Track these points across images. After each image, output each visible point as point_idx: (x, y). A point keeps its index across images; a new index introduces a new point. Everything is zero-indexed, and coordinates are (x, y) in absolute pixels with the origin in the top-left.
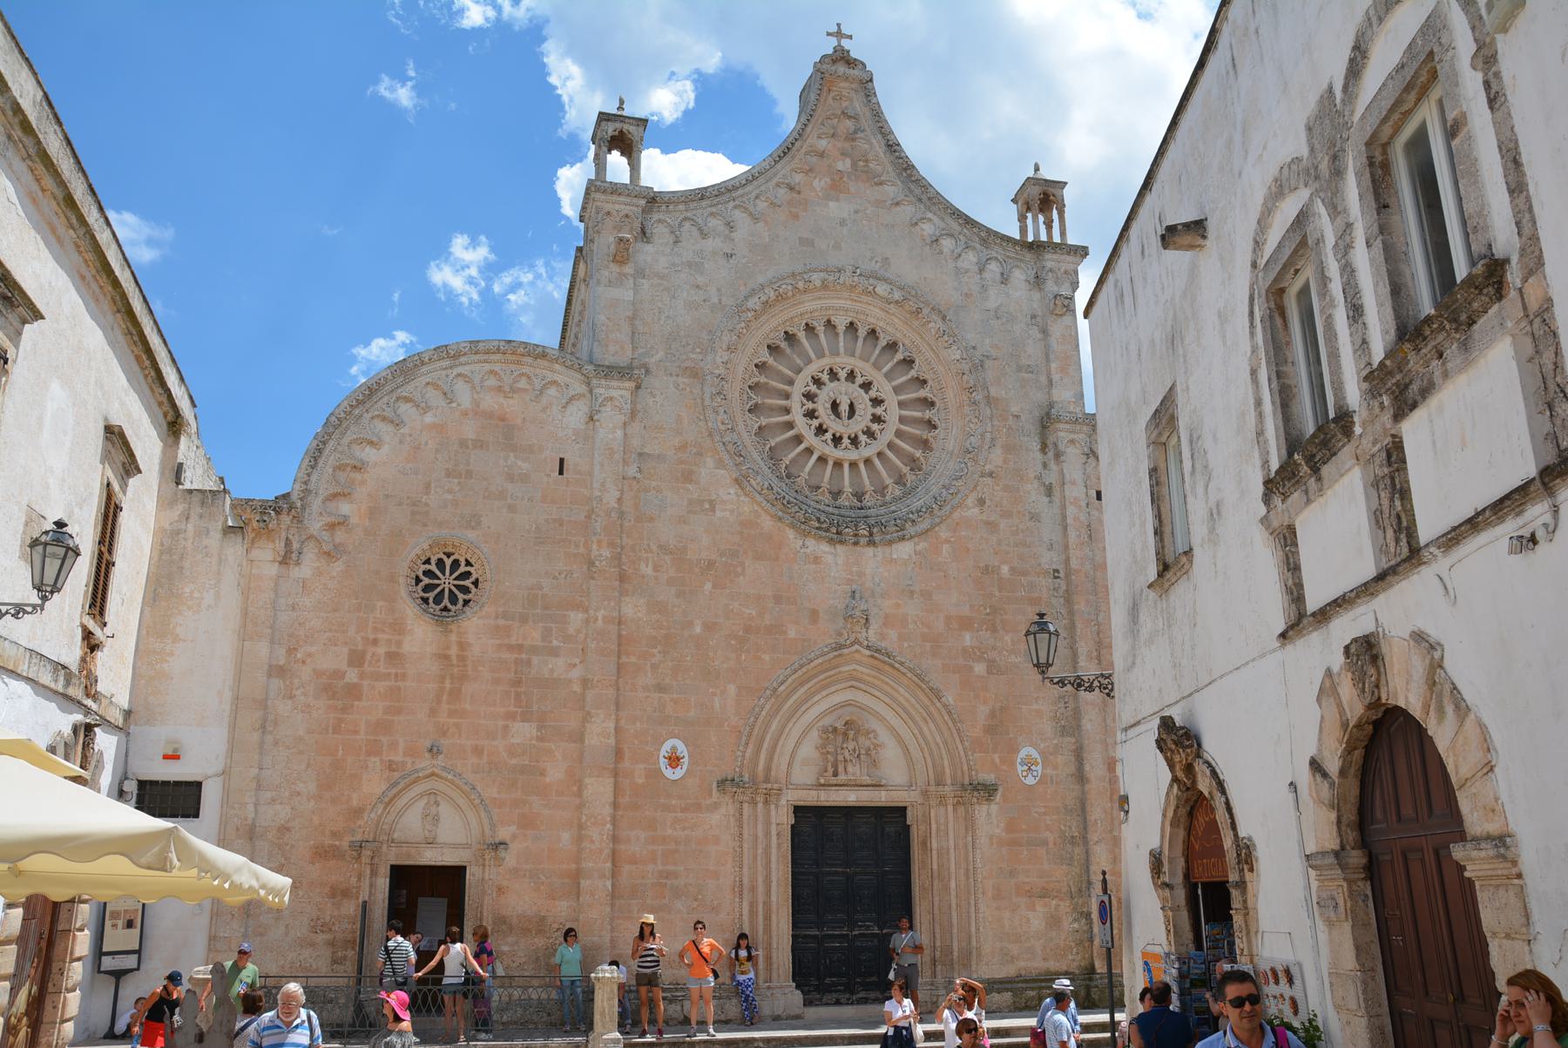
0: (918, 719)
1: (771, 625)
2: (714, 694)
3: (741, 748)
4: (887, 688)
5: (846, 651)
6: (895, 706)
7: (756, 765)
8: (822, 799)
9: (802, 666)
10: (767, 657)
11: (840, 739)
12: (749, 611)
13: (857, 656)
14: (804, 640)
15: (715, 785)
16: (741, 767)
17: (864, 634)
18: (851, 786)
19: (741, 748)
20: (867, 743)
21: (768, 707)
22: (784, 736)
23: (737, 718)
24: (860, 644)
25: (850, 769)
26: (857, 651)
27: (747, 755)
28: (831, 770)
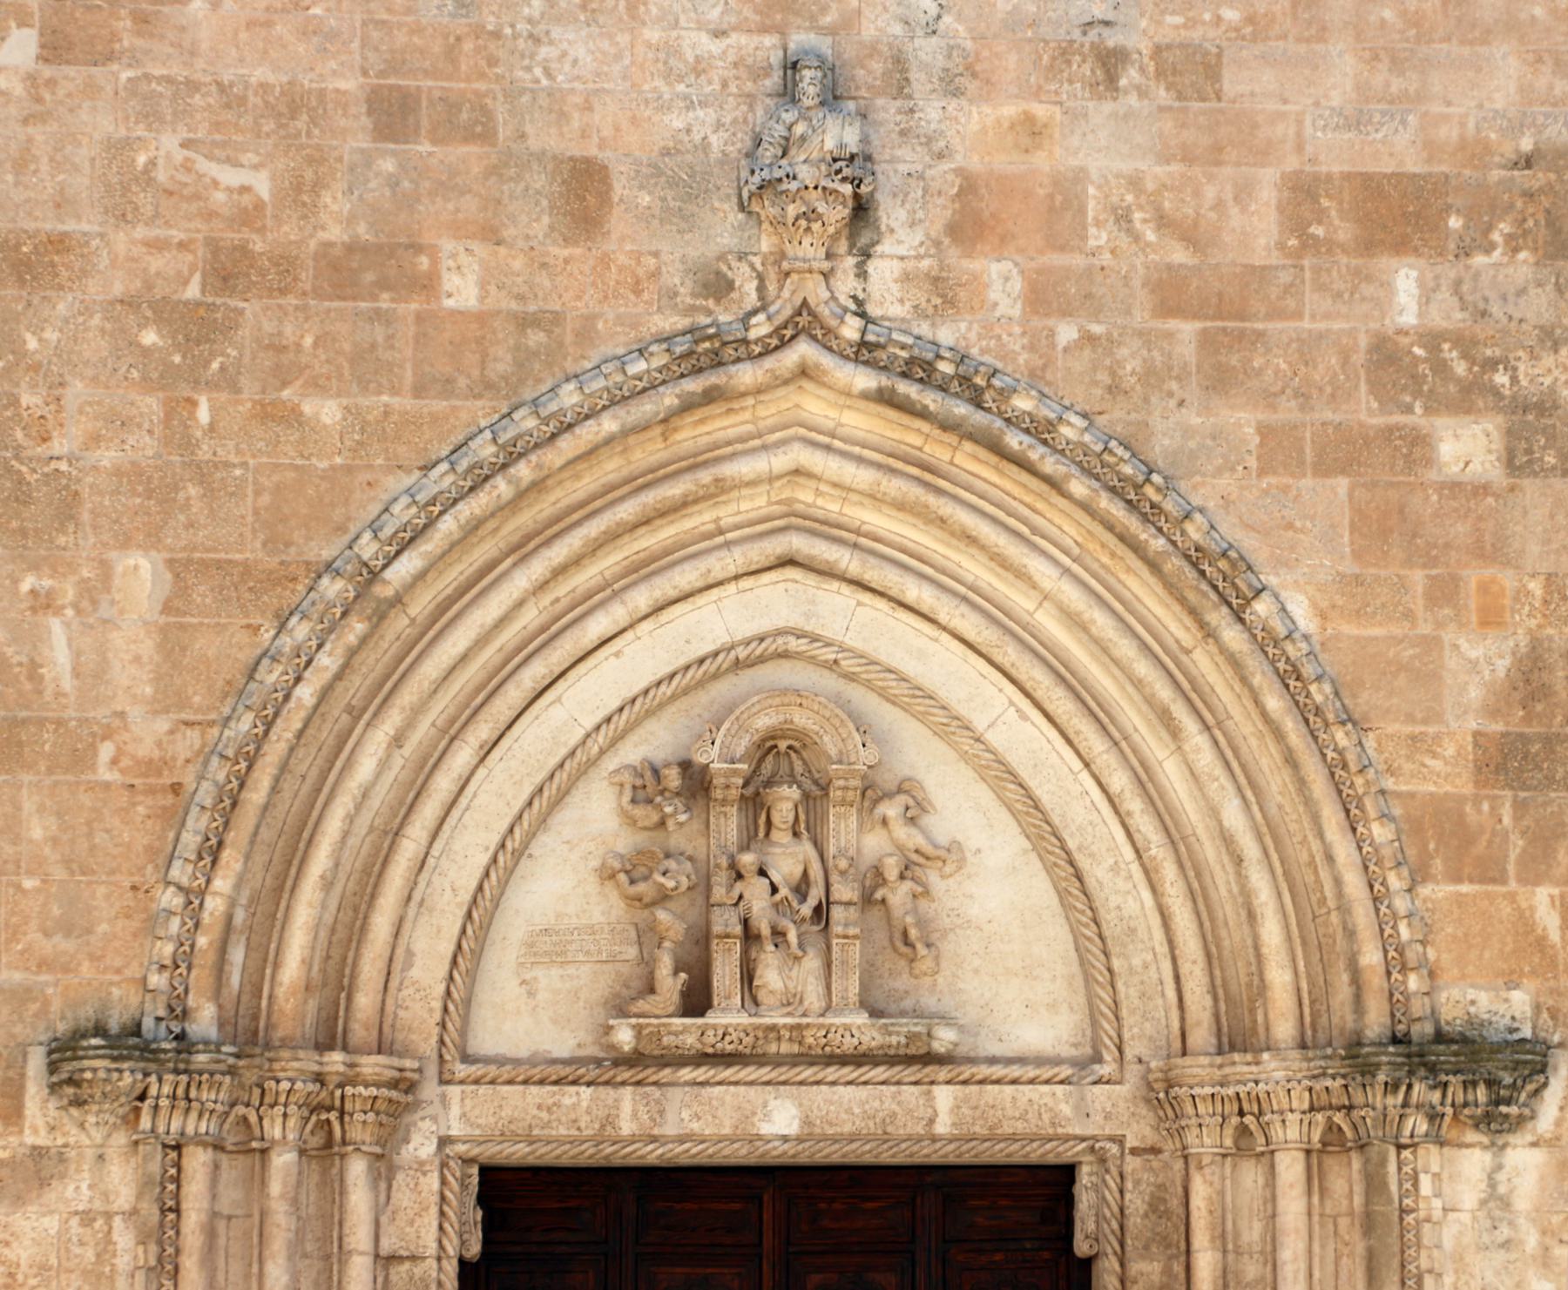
0: (1133, 717)
1: (351, 248)
2: (44, 603)
3: (179, 872)
4: (974, 568)
5: (746, 375)
6: (1010, 655)
7: (266, 958)
8: (627, 1127)
9: (511, 456)
10: (327, 412)
11: (729, 825)
12: (231, 177)
13: (814, 406)
14: (525, 322)
15: (36, 1062)
16: (182, 960)
17: (846, 285)
18: (777, 1061)
19: (179, 872)
20: (874, 844)
21: (327, 662)
22: (429, 811)
23: (162, 725)
24: (825, 338)
25: (771, 975)
26: (804, 372)
27: (214, 905)
28: (670, 985)
